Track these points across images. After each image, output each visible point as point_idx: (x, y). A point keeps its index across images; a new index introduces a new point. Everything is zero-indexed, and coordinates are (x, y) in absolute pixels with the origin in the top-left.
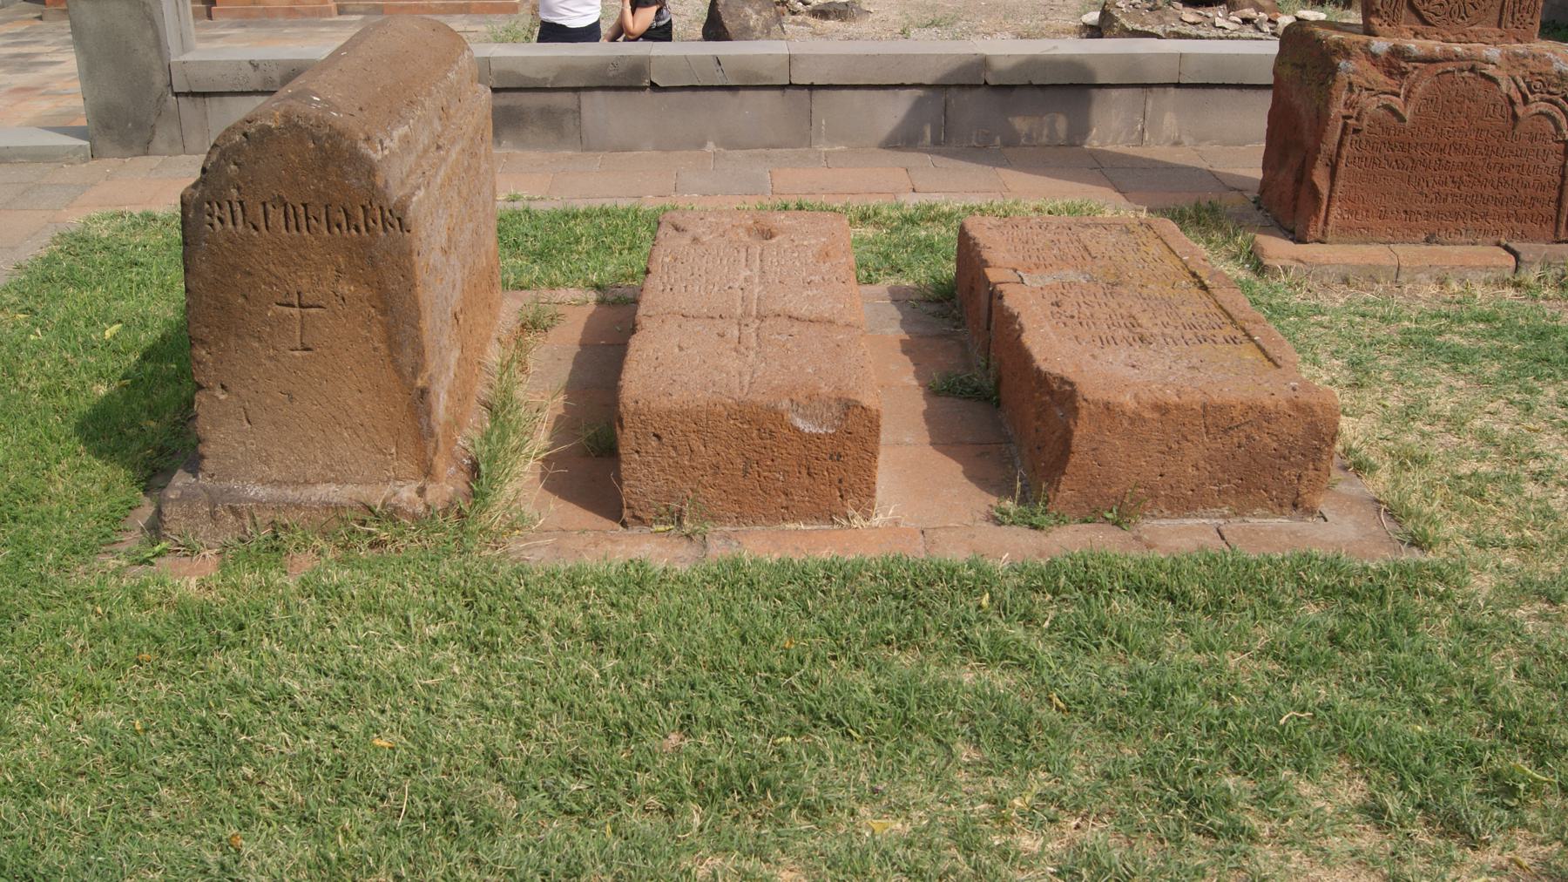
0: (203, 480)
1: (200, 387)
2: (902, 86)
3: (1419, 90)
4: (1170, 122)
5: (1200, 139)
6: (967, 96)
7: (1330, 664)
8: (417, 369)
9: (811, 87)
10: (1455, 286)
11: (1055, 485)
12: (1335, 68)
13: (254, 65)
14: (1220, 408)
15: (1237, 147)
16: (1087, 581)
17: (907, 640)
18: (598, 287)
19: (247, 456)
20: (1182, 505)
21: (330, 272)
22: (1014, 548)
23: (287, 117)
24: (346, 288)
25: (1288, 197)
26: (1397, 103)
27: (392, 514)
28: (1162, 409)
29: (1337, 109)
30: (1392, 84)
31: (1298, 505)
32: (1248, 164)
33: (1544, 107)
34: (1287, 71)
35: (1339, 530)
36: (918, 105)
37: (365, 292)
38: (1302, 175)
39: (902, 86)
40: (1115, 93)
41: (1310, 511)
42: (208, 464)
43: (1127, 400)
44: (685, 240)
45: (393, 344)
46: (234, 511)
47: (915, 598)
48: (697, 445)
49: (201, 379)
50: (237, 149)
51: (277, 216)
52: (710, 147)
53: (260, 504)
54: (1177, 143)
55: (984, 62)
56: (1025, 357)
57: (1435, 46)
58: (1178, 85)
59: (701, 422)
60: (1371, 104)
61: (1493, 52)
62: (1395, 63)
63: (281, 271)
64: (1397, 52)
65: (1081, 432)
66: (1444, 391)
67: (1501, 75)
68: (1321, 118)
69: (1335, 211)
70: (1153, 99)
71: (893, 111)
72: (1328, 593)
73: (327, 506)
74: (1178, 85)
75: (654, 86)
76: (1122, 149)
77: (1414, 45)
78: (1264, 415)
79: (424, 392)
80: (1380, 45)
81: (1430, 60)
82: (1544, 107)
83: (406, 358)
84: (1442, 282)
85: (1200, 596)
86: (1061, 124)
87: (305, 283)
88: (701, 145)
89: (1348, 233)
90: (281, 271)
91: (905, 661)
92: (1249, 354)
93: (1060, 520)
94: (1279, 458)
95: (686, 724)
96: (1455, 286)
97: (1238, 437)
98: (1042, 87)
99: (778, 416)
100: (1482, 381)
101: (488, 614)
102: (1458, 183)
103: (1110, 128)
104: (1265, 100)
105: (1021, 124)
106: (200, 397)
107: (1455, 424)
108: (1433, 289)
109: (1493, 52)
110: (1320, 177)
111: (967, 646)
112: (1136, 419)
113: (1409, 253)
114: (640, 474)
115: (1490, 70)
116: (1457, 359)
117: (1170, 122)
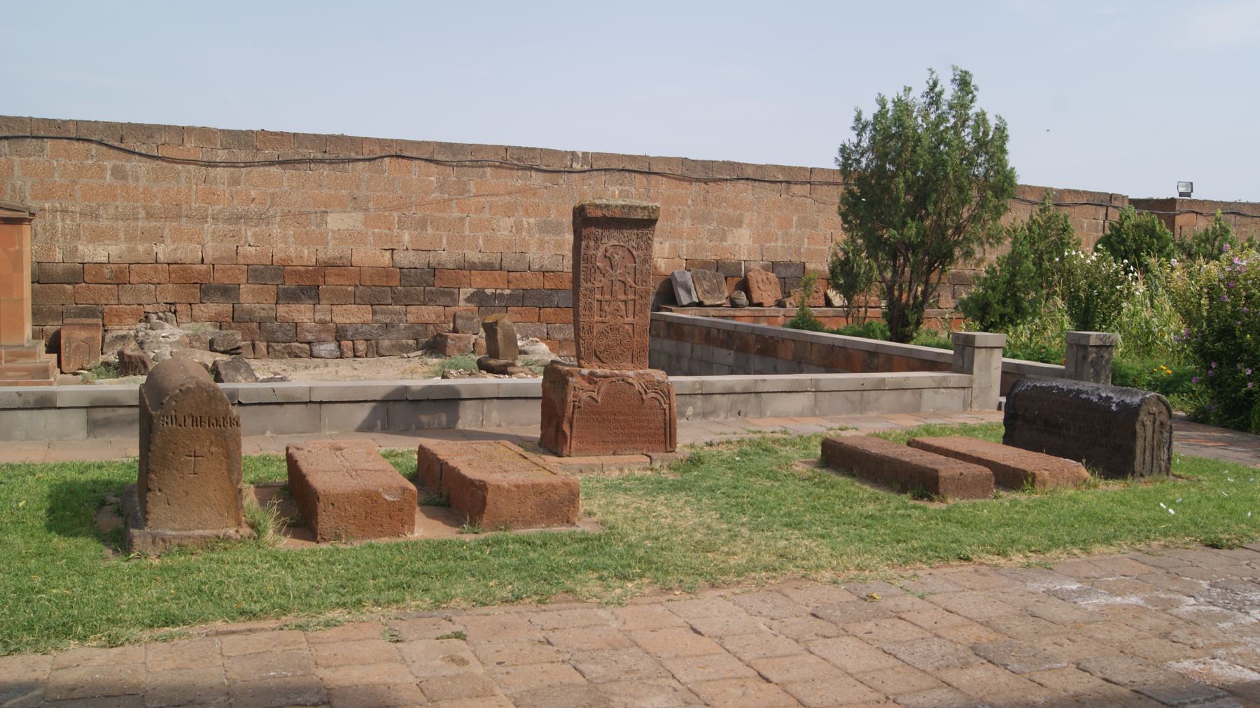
0: (147, 530)
1: (149, 490)
2: (366, 401)
3: (603, 389)
4: (495, 416)
5: (509, 424)
6: (398, 406)
7: (584, 554)
8: (238, 481)
9: (321, 403)
10: (626, 471)
11: (481, 518)
12: (567, 382)
13: (19, 394)
14: (538, 485)
15: (530, 422)
16: (498, 542)
17: (441, 557)
18: (252, 483)
19: (165, 519)
20: (528, 524)
21: (208, 443)
22: (468, 538)
23: (197, 383)
24: (213, 449)
25: (552, 441)
26: (594, 395)
27: (227, 539)
28: (518, 486)
29: (570, 398)
30: (591, 387)
31: (569, 522)
32: (535, 432)
33: (654, 395)
34: (548, 385)
35: (584, 527)
36: (374, 410)
37: (221, 450)
38: (559, 429)
39: (366, 401)
40: (468, 403)
41: (574, 524)
42: (150, 523)
43: (505, 484)
44: (305, 452)
45: (229, 470)
46: (163, 540)
47: (438, 549)
48: (348, 507)
49: (151, 486)
50: (177, 396)
51: (189, 421)
52: (268, 434)
53: (174, 537)
54: (499, 426)
55: (406, 388)
56: (464, 477)
57: (608, 371)
58: (498, 398)
59: (349, 498)
60: (584, 396)
61: (631, 373)
62: (592, 378)
63: (188, 442)
64: (592, 374)
65: (489, 496)
66: (622, 499)
67: (634, 382)
68: (564, 402)
69: (574, 443)
70: (486, 404)
71: (362, 413)
72: (581, 541)
73: (202, 537)
74: (498, 398)
75: (240, 403)
76: (474, 429)
77: (599, 371)
78: (553, 487)
79: (240, 490)
80: (585, 371)
81: (606, 377)
82: (654, 395)
83: (235, 477)
84: (621, 470)
85: (539, 542)
86: (444, 418)
87: (197, 447)
88: (263, 432)
89: (580, 452)
90: (188, 442)
91: (441, 563)
92: (546, 473)
93: (484, 531)
94: (559, 505)
95: (374, 578)
96: (626, 471)
97: (545, 496)
98: (434, 400)
99: (378, 494)
100: (636, 496)
101: (285, 561)
102: (623, 429)
103: (468, 418)
104: (540, 402)
105: (424, 418)
106: (150, 494)
107: (626, 506)
108: (617, 473)
109: (631, 373)
110: (566, 428)
111: (463, 558)
112: (509, 491)
113: (607, 459)
114: (325, 520)
115: (630, 380)
116: (626, 490)
117: (495, 416)
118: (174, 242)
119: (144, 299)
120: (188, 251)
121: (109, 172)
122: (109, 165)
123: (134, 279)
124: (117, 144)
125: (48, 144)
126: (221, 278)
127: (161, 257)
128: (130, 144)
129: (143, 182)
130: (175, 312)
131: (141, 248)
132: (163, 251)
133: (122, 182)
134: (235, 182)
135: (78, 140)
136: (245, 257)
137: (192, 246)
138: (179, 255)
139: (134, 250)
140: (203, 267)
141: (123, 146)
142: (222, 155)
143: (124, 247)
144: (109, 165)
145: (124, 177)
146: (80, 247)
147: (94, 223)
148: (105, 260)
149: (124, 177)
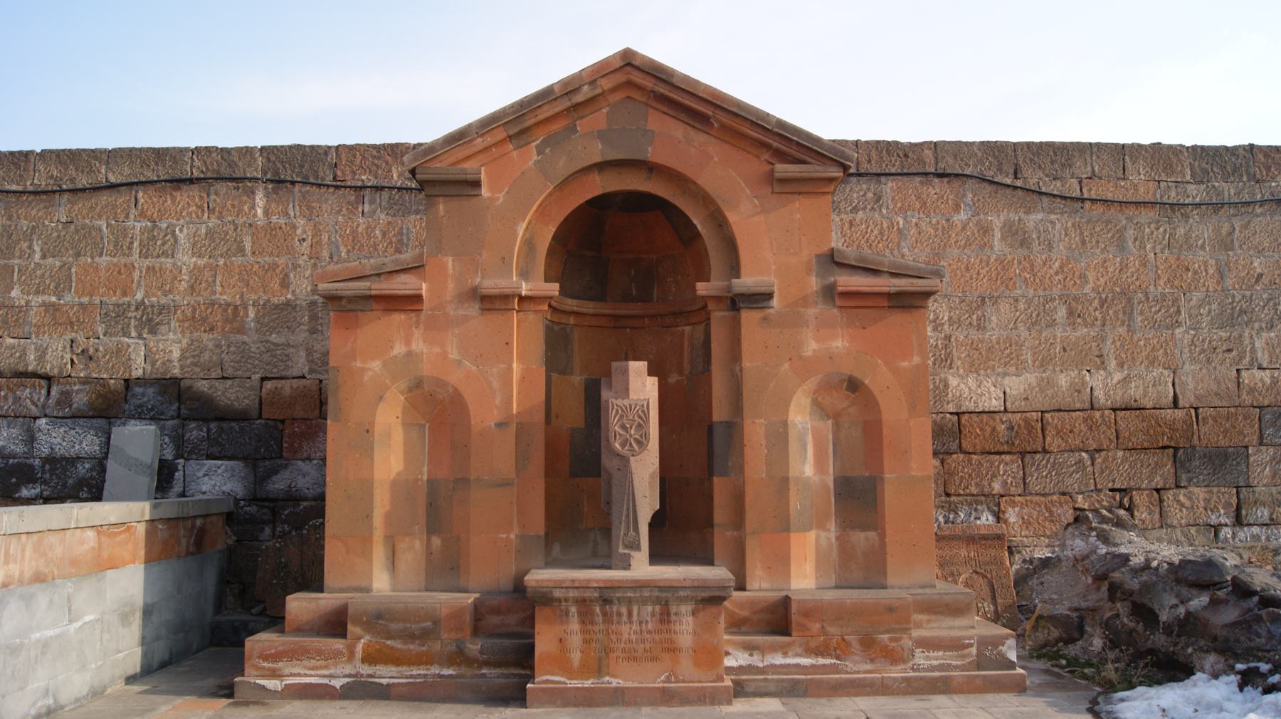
118: (1121, 365)
119: (1072, 483)
120: (1149, 385)
121: (998, 235)
122: (997, 221)
123: (1053, 442)
124: (1008, 181)
125: (889, 186)
126: (1209, 435)
127: (1099, 394)
128: (1032, 178)
129: (1060, 250)
130: (1130, 510)
131: (1063, 380)
132: (1105, 384)
133: (1023, 252)
134: (1226, 244)
135: (941, 176)
136: (1252, 391)
137: (1156, 372)
138: (1135, 392)
139: (1050, 383)
140: (1179, 414)
141: (1019, 183)
142: (1196, 193)
143: (1031, 378)
144: (997, 221)
145: (1025, 243)
146: (953, 382)
147: (975, 335)
148: (996, 404)
149: (1025, 243)
